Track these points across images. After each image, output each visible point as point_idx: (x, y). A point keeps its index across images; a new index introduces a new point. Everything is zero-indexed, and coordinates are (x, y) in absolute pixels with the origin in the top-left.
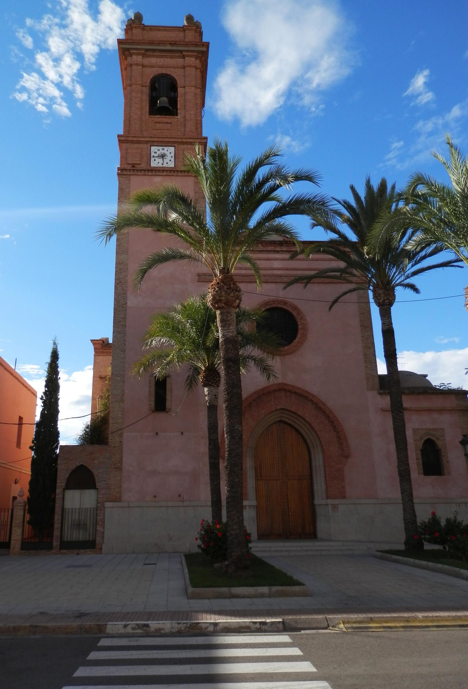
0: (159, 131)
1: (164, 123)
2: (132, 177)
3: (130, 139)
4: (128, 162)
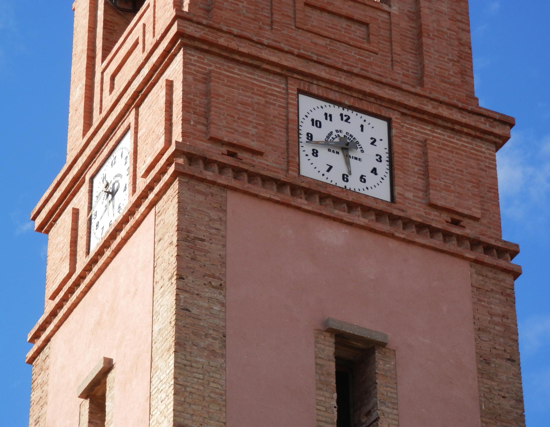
0: (321, 42)
1: (340, 16)
2: (233, 199)
3: (222, 41)
4: (215, 132)
